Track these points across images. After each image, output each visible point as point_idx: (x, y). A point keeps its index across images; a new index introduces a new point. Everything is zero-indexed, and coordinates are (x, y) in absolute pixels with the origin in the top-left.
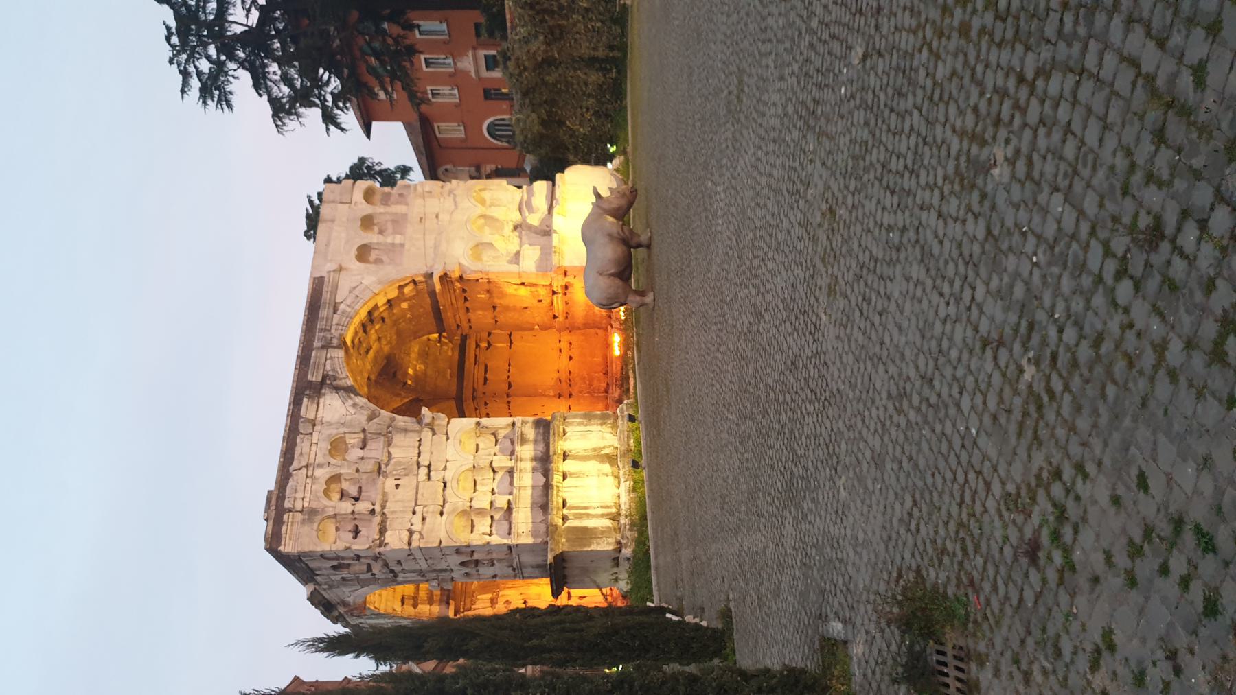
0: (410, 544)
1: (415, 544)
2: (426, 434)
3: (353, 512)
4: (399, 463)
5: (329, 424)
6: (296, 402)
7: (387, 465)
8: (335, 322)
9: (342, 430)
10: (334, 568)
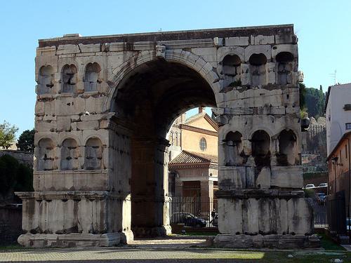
2: (99, 117)
7: (82, 97)
8: (175, 51)
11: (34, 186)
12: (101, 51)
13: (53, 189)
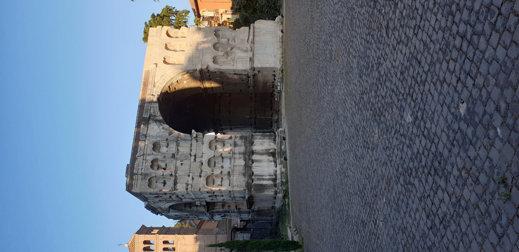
0: (187, 189)
1: (189, 189)
2: (194, 141)
3: (163, 175)
4: (183, 154)
5: (153, 137)
6: (138, 126)
9: (158, 139)
10: (155, 197)
11: (242, 189)
12: (145, 141)
13: (244, 175)
